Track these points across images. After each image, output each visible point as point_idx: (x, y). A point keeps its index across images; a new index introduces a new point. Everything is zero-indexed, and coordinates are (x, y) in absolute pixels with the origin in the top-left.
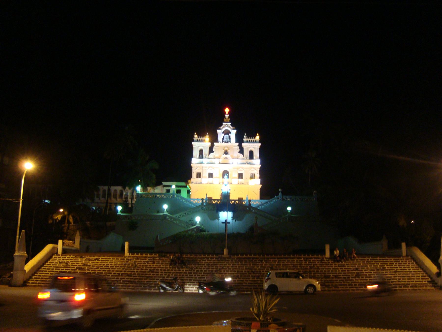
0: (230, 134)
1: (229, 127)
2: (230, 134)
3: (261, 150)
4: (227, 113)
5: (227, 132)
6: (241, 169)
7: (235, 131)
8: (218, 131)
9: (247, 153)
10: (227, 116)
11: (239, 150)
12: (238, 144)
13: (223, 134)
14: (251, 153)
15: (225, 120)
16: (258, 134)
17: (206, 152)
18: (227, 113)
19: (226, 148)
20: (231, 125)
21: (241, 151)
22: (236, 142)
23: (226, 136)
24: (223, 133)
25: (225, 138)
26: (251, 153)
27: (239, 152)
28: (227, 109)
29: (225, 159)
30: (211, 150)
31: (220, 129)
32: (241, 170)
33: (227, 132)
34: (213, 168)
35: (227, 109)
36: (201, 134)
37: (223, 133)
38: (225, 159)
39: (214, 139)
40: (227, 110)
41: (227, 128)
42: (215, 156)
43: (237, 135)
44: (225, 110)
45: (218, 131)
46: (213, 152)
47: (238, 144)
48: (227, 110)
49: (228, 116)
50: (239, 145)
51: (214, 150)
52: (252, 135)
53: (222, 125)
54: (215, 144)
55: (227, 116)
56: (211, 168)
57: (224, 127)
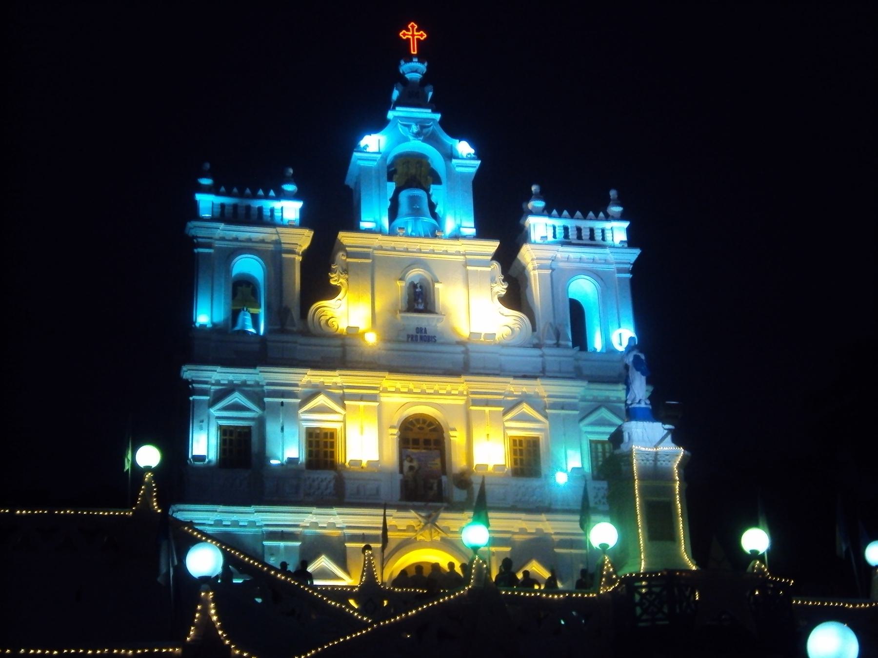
0: (433, 188)
2: (433, 188)
4: (414, 52)
6: (526, 409)
10: (413, 70)
11: (501, 288)
12: (491, 246)
13: (391, 187)
16: (613, 193)
18: (414, 52)
19: (415, 274)
22: (483, 233)
23: (404, 196)
29: (412, 338)
34: (341, 400)
36: (249, 178)
37: (390, 179)
38: (412, 338)
39: (331, 211)
44: (403, 35)
47: (491, 246)
48: (413, 34)
49: (423, 67)
50: (497, 256)
52: (575, 198)
54: (345, 238)
56: (321, 400)
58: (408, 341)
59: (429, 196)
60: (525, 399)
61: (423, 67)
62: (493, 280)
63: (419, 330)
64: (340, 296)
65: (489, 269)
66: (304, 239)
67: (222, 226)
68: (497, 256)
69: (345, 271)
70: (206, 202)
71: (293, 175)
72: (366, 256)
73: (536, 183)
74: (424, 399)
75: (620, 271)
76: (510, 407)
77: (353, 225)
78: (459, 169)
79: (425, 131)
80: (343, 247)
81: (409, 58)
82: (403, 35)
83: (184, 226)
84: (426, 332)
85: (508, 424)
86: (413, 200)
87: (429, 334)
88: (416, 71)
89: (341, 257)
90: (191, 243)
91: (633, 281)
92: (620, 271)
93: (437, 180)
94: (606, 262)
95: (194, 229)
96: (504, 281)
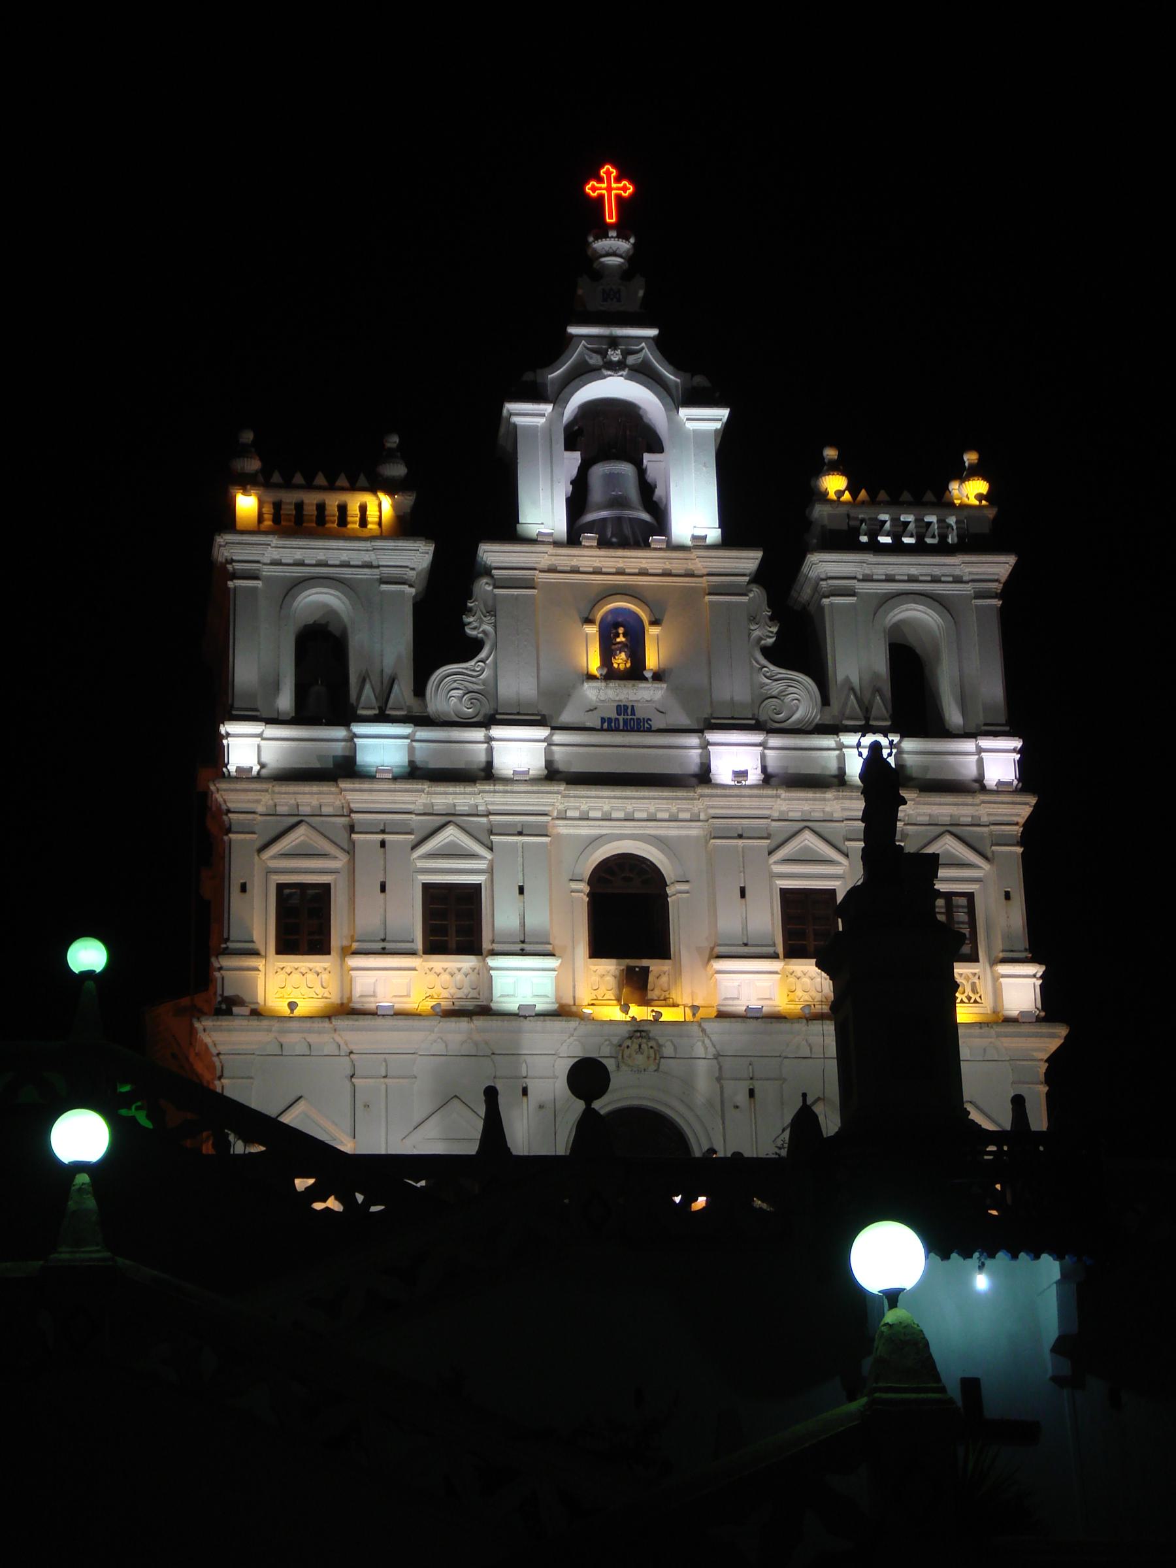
0: (647, 458)
1: (643, 373)
2: (647, 458)
3: (1025, 624)
4: (611, 218)
5: (610, 438)
6: (808, 840)
7: (708, 420)
9: (857, 661)
11: (768, 633)
12: (749, 560)
14: (909, 668)
17: (384, 644)
18: (611, 218)
20: (659, 343)
21: (799, 643)
24: (573, 437)
25: (597, 493)
26: (909, 668)
27: (776, 655)
28: (608, 170)
30: (442, 632)
31: (536, 394)
32: (806, 858)
33: (610, 438)
34: (485, 837)
35: (608, 170)
37: (570, 446)
38: (608, 725)
39: (466, 504)
41: (615, 387)
42: (488, 692)
43: (734, 463)
44: (592, 189)
45: (528, 416)
46: (469, 649)
47: (749, 560)
48: (609, 187)
51: (476, 625)
53: (565, 343)
54: (492, 554)
55: (613, 249)
57: (584, 373)
58: (602, 730)
59: (641, 472)
60: (807, 824)
61: (624, 246)
62: (753, 619)
63: (622, 709)
64: (482, 655)
65: (745, 599)
66: (417, 556)
67: (274, 540)
68: (759, 577)
69: (492, 612)
70: (246, 504)
71: (400, 446)
72: (529, 584)
73: (831, 445)
74: (629, 828)
75: (979, 595)
77: (506, 527)
78: (690, 426)
79: (631, 360)
80: (487, 571)
81: (602, 231)
82: (592, 189)
83: (209, 544)
84: (633, 713)
85: (777, 869)
86: (612, 480)
87: (639, 714)
88: (614, 254)
89: (483, 586)
90: (225, 573)
91: (1002, 610)
92: (979, 595)
93: (656, 446)
94: (958, 580)
95: (227, 548)
96: (771, 618)
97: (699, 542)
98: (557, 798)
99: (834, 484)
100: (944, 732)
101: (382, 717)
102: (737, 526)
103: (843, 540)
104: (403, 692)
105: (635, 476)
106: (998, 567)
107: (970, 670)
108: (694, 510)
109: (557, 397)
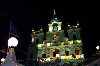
1: (56, 21)
6: (67, 48)
7: (60, 23)
8: (49, 25)
10: (54, 14)
15: (53, 17)
17: (41, 40)
20: (57, 19)
29: (54, 42)
33: (55, 25)
38: (54, 42)
40: (54, 11)
41: (55, 22)
42: (47, 41)
45: (49, 25)
47: (63, 31)
54: (47, 33)
55: (54, 14)
57: (53, 21)
60: (67, 47)
63: (55, 41)
76: (65, 48)
97: (59, 30)
98: (51, 47)
99: (69, 25)
100: (76, 40)
101: (40, 44)
102: (62, 29)
103: (70, 29)
104: (42, 42)
105: (54, 27)
106: (80, 29)
107: (78, 35)
108: (60, 28)
109: (51, 23)
